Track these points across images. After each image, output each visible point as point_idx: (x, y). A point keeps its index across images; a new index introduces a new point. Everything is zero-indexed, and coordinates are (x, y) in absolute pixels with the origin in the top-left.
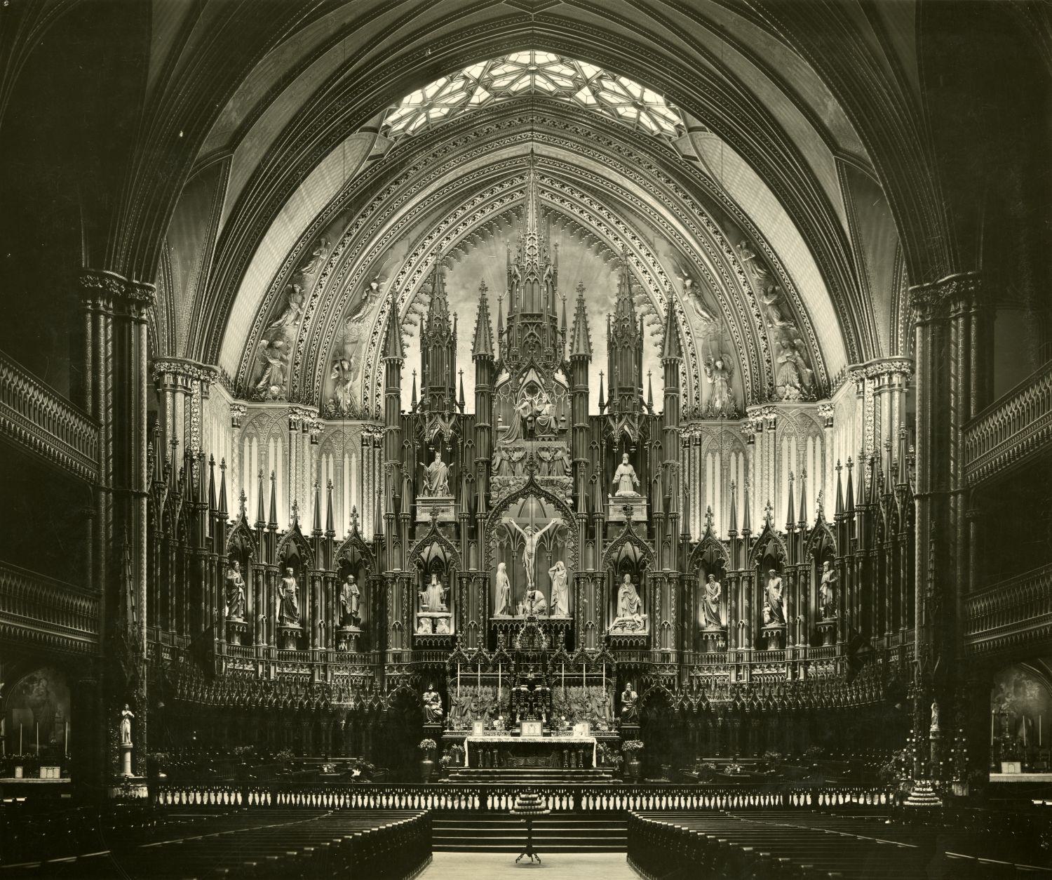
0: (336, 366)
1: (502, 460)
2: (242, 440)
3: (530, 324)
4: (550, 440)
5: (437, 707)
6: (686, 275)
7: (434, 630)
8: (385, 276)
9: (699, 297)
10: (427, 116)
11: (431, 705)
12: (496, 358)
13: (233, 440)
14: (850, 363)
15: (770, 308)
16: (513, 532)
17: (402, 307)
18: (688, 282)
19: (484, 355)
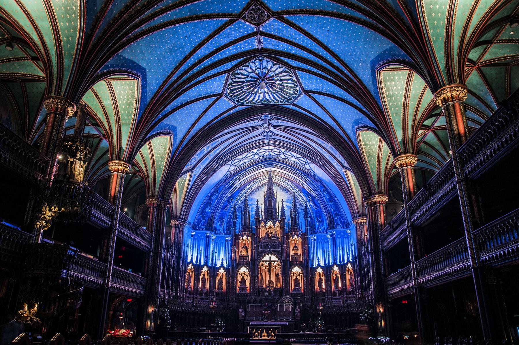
2: (194, 240)
7: (243, 291)
8: (233, 199)
10: (242, 156)
12: (261, 219)
17: (237, 206)
18: (311, 200)
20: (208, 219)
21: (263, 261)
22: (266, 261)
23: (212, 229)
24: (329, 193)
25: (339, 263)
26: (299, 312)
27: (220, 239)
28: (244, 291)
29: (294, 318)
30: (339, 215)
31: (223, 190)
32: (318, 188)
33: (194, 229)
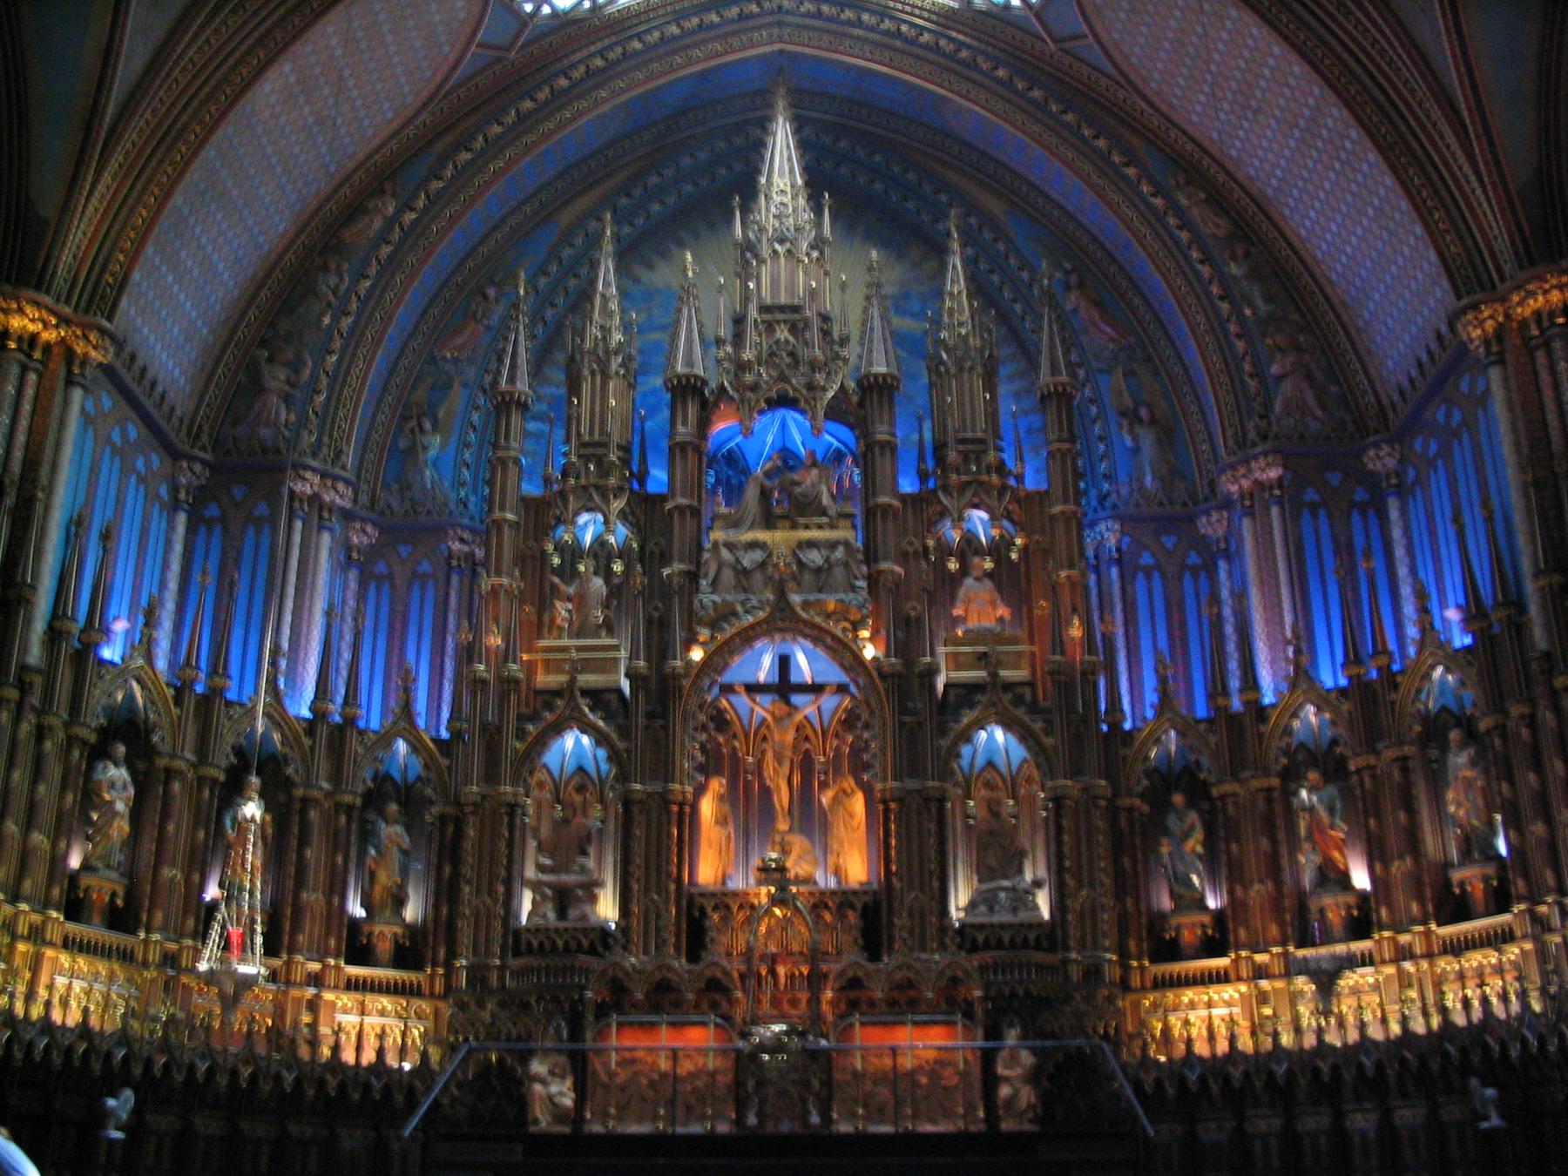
0: (413, 423)
1: (721, 566)
2: (191, 531)
3: (778, 322)
4: (820, 527)
5: (563, 1092)
6: (1068, 266)
7: (562, 913)
9: (1098, 305)
11: (544, 1082)
13: (171, 527)
14: (1459, 297)
15: (1244, 283)
16: (746, 722)
18: (1074, 279)
19: (688, 377)
20: (315, 378)
21: (728, 689)
22: (753, 689)
23: (339, 454)
24: (1217, 201)
25: (1343, 682)
26: (1034, 1077)
27: (404, 550)
28: (573, 913)
29: (992, 1117)
30: (1298, 349)
31: (436, 185)
32: (1131, 171)
33: (203, 448)
